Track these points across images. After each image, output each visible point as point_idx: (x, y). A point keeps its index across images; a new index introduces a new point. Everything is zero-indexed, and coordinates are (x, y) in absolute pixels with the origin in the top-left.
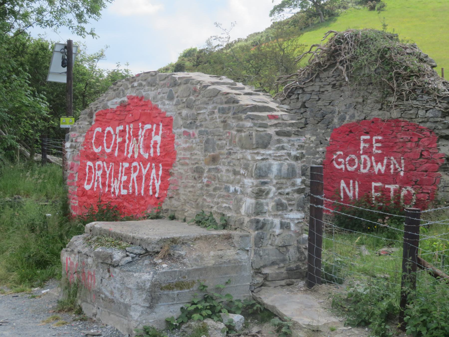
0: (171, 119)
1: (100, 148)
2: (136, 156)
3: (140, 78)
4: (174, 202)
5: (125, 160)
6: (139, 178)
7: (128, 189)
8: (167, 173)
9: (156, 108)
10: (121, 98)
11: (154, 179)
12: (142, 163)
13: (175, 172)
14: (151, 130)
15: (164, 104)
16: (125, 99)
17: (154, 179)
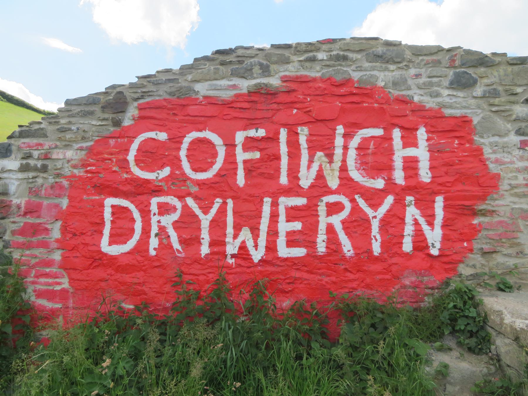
0: (464, 122)
1: (166, 171)
2: (333, 183)
3: (337, 46)
4: (499, 259)
5: (293, 189)
6: (357, 225)
7: (311, 245)
8: (461, 213)
9: (404, 101)
10: (255, 78)
11: (416, 223)
12: (362, 196)
13: (501, 210)
14: (388, 138)
15: (438, 95)
16: (275, 82)
17: (416, 223)
